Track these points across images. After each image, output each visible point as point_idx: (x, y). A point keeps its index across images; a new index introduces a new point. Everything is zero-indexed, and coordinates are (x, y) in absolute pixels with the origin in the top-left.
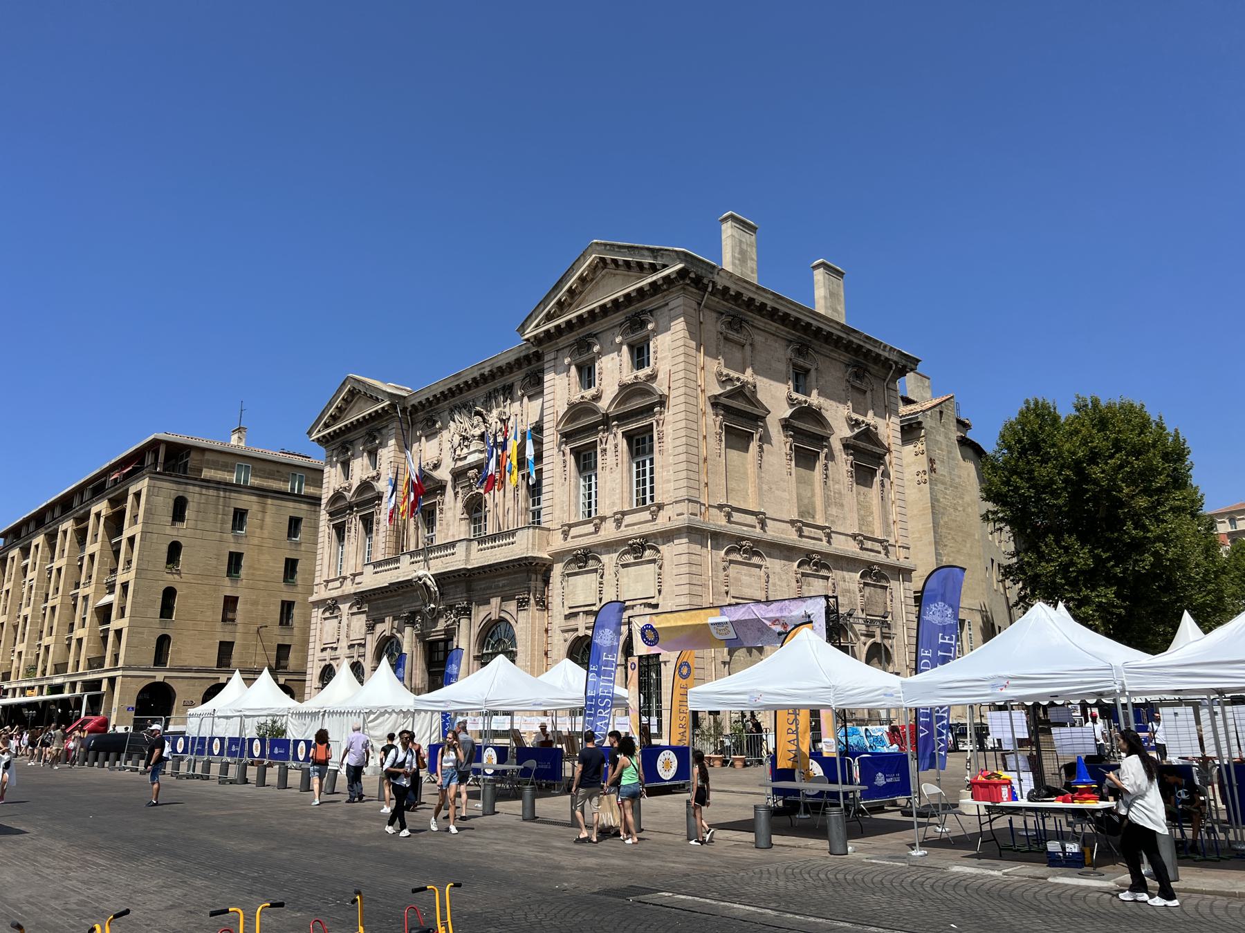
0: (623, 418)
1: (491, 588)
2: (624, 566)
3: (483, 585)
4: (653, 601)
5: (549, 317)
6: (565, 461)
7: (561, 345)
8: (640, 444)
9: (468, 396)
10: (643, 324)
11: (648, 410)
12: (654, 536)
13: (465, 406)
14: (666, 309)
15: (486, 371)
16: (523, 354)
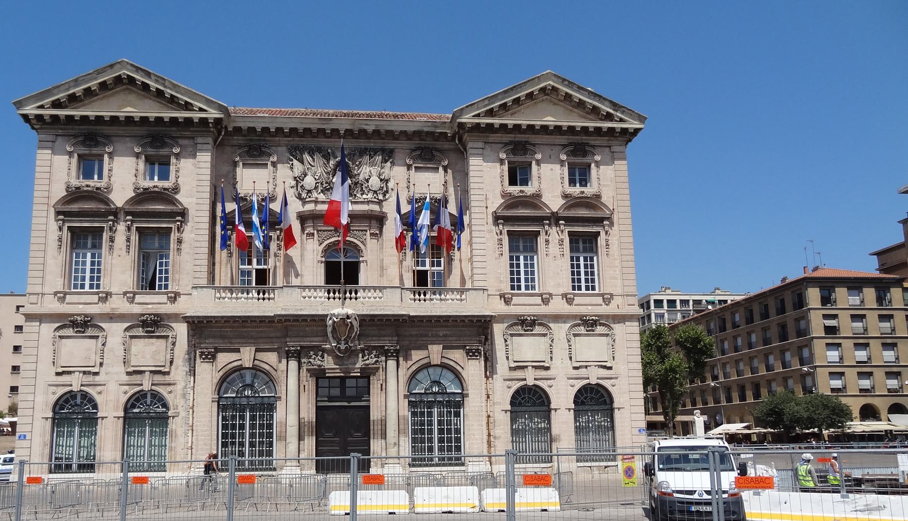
0: (570, 221)
1: (427, 336)
2: (575, 335)
3: (414, 332)
4: (608, 365)
5: (490, 113)
6: (501, 240)
7: (491, 139)
8: (584, 244)
9: (323, 142)
10: (585, 154)
11: (599, 221)
12: (607, 317)
13: (319, 150)
14: (608, 149)
15: (370, 128)
16: (426, 129)
